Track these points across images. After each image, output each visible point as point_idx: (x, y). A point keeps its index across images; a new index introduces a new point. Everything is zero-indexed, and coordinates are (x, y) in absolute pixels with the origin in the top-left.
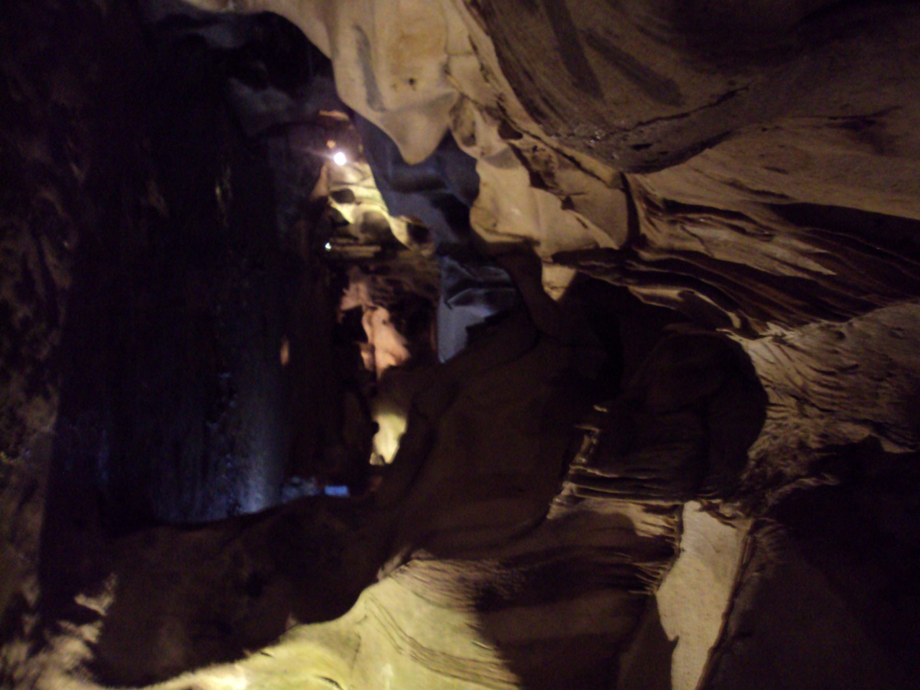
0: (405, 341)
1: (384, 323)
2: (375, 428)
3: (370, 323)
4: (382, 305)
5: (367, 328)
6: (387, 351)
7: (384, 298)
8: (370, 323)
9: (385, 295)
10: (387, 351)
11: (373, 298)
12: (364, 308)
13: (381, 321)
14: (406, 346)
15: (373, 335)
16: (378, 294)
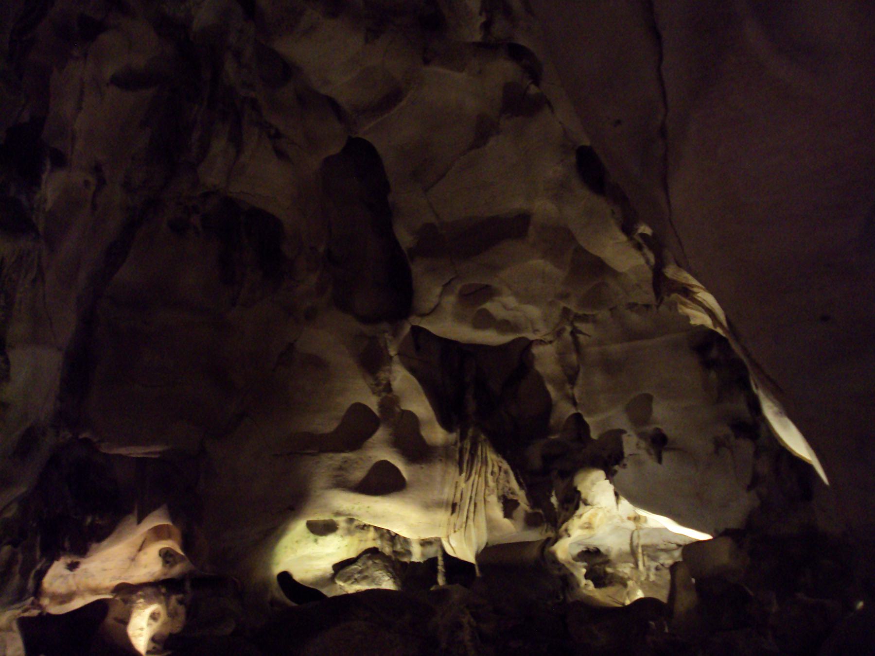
0: (133, 519)
1: (72, 566)
2: (285, 577)
3: (69, 597)
4: (42, 574)
5: (78, 603)
6: (133, 559)
7: (25, 575)
8: (69, 597)
9: (17, 568)
10: (133, 559)
11: (20, 596)
12: (35, 612)
13: (67, 572)
14: (140, 521)
15: (95, 591)
16: (16, 580)
